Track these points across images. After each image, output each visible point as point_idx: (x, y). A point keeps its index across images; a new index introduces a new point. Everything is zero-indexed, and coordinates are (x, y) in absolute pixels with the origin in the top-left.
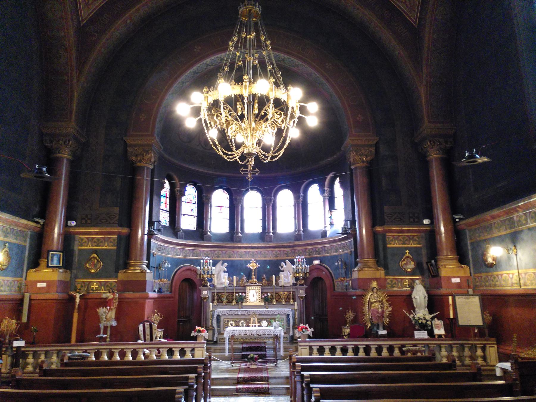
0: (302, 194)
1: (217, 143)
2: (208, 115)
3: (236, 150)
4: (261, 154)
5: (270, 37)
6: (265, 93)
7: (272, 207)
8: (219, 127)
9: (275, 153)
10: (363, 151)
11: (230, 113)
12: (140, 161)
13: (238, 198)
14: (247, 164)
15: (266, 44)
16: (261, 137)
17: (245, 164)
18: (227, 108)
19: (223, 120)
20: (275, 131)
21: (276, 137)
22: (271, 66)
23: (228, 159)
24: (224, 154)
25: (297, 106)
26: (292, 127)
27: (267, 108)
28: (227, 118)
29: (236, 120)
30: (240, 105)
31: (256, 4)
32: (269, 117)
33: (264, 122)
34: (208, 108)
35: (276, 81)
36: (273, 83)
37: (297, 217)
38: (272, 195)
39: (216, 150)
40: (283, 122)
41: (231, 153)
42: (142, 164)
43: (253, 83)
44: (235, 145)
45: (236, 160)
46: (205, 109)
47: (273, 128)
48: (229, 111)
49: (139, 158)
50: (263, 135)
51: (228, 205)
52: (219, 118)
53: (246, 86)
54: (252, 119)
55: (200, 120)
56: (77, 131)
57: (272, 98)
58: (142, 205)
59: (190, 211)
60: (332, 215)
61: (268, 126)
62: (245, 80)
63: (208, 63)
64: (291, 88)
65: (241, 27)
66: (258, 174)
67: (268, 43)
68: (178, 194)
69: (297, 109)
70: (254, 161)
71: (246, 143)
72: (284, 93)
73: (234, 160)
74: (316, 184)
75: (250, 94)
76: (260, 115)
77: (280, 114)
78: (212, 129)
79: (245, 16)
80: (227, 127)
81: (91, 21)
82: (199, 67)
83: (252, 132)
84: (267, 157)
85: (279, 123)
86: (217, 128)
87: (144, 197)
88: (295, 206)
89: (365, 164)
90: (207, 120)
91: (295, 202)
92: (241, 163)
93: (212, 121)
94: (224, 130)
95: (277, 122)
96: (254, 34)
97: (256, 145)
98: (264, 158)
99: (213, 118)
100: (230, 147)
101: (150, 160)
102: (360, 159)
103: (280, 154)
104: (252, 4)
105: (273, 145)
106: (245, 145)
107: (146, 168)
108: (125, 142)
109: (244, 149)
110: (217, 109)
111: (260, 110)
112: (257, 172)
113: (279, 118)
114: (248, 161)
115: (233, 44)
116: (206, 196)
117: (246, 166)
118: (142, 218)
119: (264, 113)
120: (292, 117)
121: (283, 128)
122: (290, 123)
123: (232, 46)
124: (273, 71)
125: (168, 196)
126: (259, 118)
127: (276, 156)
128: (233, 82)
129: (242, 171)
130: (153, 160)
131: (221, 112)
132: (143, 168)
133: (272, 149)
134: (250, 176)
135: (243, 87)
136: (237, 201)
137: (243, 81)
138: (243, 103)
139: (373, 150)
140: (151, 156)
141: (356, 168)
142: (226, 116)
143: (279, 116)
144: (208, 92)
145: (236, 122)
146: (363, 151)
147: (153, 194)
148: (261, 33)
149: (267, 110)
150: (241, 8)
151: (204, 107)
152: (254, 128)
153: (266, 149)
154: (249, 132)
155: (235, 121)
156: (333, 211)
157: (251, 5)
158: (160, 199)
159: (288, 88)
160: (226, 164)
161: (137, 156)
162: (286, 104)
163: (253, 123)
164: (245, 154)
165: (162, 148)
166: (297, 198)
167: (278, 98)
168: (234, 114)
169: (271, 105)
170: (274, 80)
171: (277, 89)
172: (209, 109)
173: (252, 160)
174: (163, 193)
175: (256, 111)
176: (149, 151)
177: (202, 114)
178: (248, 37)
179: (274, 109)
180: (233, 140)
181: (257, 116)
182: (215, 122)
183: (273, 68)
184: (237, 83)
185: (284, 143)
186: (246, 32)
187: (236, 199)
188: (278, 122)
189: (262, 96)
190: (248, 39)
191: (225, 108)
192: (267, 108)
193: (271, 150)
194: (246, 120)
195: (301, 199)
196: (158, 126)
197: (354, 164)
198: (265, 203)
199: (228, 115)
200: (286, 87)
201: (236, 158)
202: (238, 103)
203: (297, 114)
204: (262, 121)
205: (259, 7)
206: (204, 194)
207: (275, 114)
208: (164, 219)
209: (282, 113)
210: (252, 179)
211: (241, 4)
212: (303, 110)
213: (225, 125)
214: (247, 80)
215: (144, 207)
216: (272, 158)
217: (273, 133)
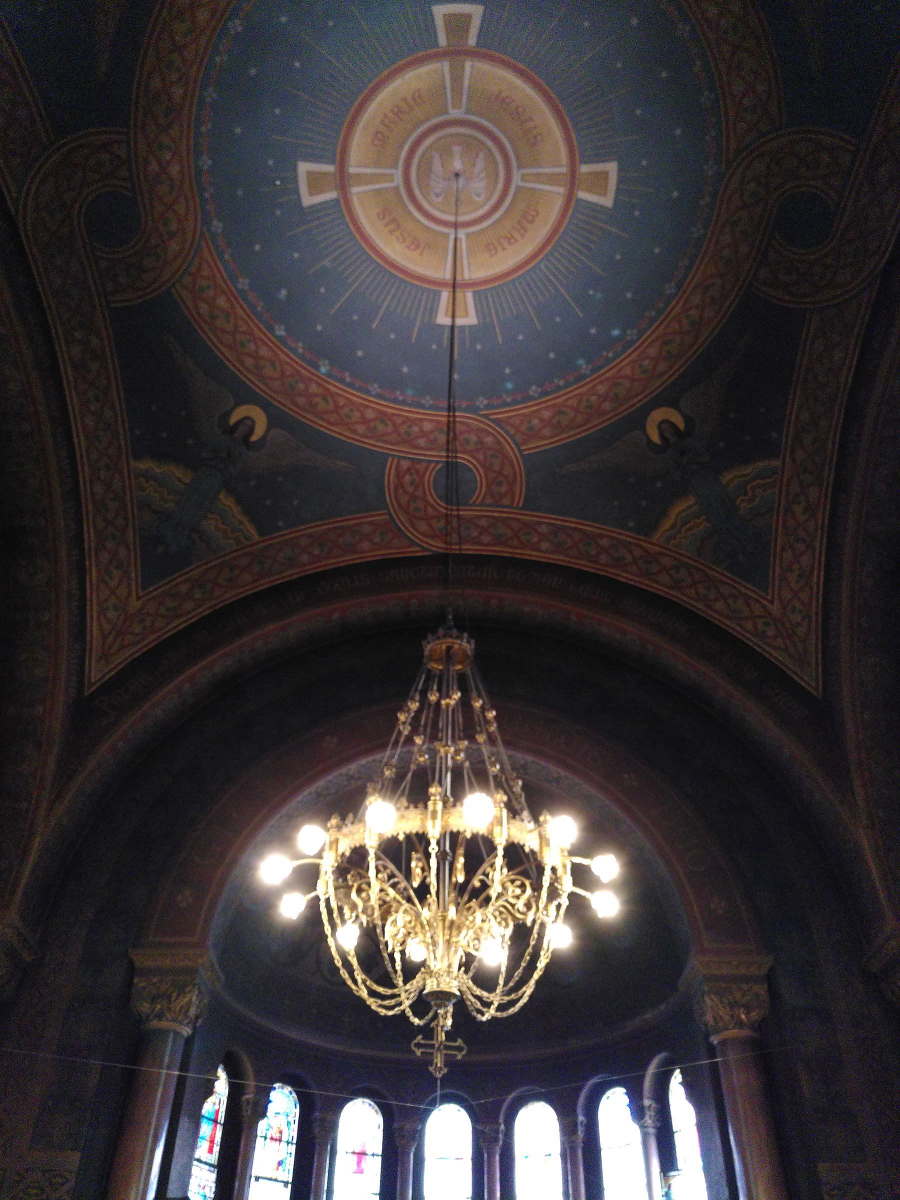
0: (581, 1118)
1: (354, 962)
2: (336, 888)
3: (405, 982)
4: (472, 994)
5: (495, 699)
6: (482, 830)
7: (501, 1155)
8: (364, 919)
9: (509, 993)
10: (738, 995)
11: (392, 881)
12: (160, 1016)
13: (408, 1126)
14: (433, 1025)
15: (485, 717)
16: (471, 945)
17: (427, 1025)
18: (385, 868)
19: (374, 901)
20: (509, 931)
21: (510, 947)
22: (498, 767)
23: (380, 1010)
24: (372, 993)
25: (565, 866)
26: (553, 922)
27: (489, 870)
28: (383, 894)
29: (409, 900)
30: (419, 860)
31: (462, 636)
32: (493, 892)
33: (481, 906)
34: (338, 867)
35: (509, 800)
36: (502, 805)
37: (571, 1192)
38: (501, 1120)
39: (350, 982)
40: (528, 906)
41: (389, 992)
42: (164, 1024)
43: (454, 805)
44: (402, 970)
45: (403, 1011)
46: (330, 870)
47: (504, 923)
48: (391, 876)
49: (158, 1007)
50: (476, 942)
51: (379, 1151)
52: (364, 895)
53: (434, 813)
54: (450, 896)
55: (317, 899)
56: (20, 934)
57: (500, 843)
58: (146, 1146)
59: (276, 1165)
60: (669, 1187)
61: (492, 918)
62: (432, 798)
63: (351, 773)
64: (549, 817)
65: (426, 681)
66: (464, 1056)
67: (492, 714)
68: (247, 1112)
69: (565, 872)
70: (453, 1017)
71: (431, 963)
72: (530, 831)
73: (396, 1011)
74: (625, 1088)
75: (445, 833)
76: (469, 888)
77: (523, 886)
78: (346, 926)
79: (437, 661)
80: (384, 918)
81: (108, 687)
82: (330, 782)
83: (447, 932)
84: (488, 1005)
85: (518, 910)
86: (359, 921)
87: (154, 1120)
88: (564, 1156)
89: (746, 1032)
90: (334, 905)
91: (563, 1143)
92: (416, 1021)
93: (348, 904)
94: (375, 926)
95: (513, 906)
96: (457, 696)
97: (459, 969)
98: (479, 1005)
99: (348, 896)
100: (387, 972)
101: (187, 1011)
102: (732, 1016)
103: (523, 995)
104: (454, 636)
105: (503, 969)
106: (429, 967)
107: (172, 1035)
108: (131, 962)
109: (424, 979)
110: (360, 871)
111: (470, 870)
112: (459, 1049)
113: (518, 897)
114: (436, 1016)
115: (407, 718)
116: (323, 1120)
117: (428, 1032)
118: (138, 1187)
119: (482, 881)
120: (553, 894)
121: (529, 923)
122: (547, 910)
123: (404, 723)
124: (501, 778)
125: (221, 1117)
126: (466, 897)
127: (513, 1003)
128: (404, 802)
129: (418, 1045)
130: (193, 1011)
131: (369, 878)
132: (164, 1033)
133: (501, 981)
134: (439, 1061)
135: (427, 814)
136: (403, 1137)
137: (429, 800)
138: (428, 856)
139: (761, 989)
140: (191, 1000)
141: (723, 1043)
142: (382, 890)
143: (518, 891)
144: (339, 828)
145: (406, 905)
146: (738, 995)
147: (179, 1112)
148: (474, 694)
149: (487, 876)
150: (429, 643)
151: (328, 864)
152: (452, 922)
153: (486, 980)
154: (440, 932)
155: (404, 902)
156: (672, 1173)
157: (451, 637)
158: (197, 1126)
159: (542, 819)
160: (380, 1025)
161: (154, 999)
162: (536, 859)
163: (452, 910)
164: (427, 994)
165: (223, 978)
166: (568, 1129)
167: (516, 841)
168: (403, 884)
169: (499, 861)
170: (505, 798)
171: (512, 821)
172: (341, 872)
173: (446, 1013)
174: (208, 1108)
175: (461, 878)
176: (188, 986)
177: (320, 884)
178: (443, 702)
179: (505, 870)
180: (397, 956)
181: (461, 889)
182: (354, 907)
183: (502, 769)
184: (412, 806)
185: (532, 966)
186: (439, 690)
187: (402, 1129)
188: (516, 907)
189: (475, 836)
190: (444, 707)
191: (381, 868)
192: (489, 870)
193: (497, 984)
194: (432, 898)
195: (581, 1133)
196: (218, 922)
197: (717, 1031)
198: (483, 1145)
199: (386, 886)
200: (535, 818)
201: (402, 1008)
202: (414, 855)
203: (567, 885)
204: (474, 903)
205: (468, 642)
206: (317, 1114)
207: (509, 884)
208: (202, 1192)
209: (527, 883)
210: (445, 1070)
211: (429, 635)
212: (581, 875)
213: (377, 913)
214: (438, 798)
215: (148, 1150)
216: (501, 1008)
217: (503, 936)
